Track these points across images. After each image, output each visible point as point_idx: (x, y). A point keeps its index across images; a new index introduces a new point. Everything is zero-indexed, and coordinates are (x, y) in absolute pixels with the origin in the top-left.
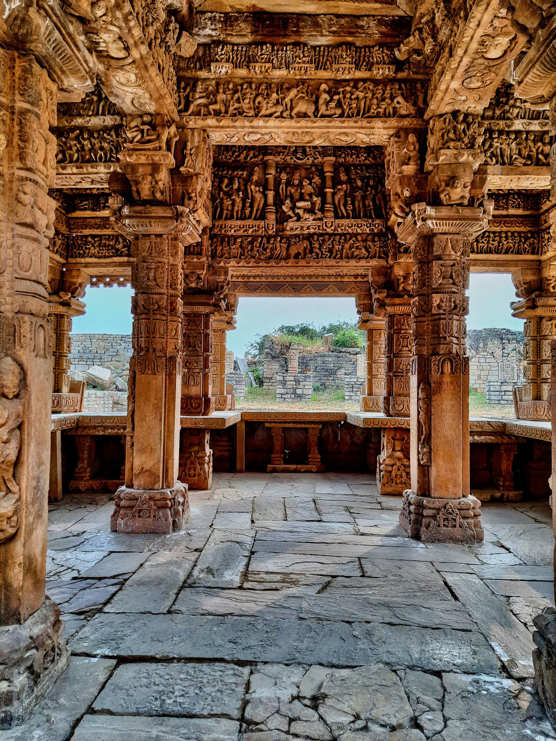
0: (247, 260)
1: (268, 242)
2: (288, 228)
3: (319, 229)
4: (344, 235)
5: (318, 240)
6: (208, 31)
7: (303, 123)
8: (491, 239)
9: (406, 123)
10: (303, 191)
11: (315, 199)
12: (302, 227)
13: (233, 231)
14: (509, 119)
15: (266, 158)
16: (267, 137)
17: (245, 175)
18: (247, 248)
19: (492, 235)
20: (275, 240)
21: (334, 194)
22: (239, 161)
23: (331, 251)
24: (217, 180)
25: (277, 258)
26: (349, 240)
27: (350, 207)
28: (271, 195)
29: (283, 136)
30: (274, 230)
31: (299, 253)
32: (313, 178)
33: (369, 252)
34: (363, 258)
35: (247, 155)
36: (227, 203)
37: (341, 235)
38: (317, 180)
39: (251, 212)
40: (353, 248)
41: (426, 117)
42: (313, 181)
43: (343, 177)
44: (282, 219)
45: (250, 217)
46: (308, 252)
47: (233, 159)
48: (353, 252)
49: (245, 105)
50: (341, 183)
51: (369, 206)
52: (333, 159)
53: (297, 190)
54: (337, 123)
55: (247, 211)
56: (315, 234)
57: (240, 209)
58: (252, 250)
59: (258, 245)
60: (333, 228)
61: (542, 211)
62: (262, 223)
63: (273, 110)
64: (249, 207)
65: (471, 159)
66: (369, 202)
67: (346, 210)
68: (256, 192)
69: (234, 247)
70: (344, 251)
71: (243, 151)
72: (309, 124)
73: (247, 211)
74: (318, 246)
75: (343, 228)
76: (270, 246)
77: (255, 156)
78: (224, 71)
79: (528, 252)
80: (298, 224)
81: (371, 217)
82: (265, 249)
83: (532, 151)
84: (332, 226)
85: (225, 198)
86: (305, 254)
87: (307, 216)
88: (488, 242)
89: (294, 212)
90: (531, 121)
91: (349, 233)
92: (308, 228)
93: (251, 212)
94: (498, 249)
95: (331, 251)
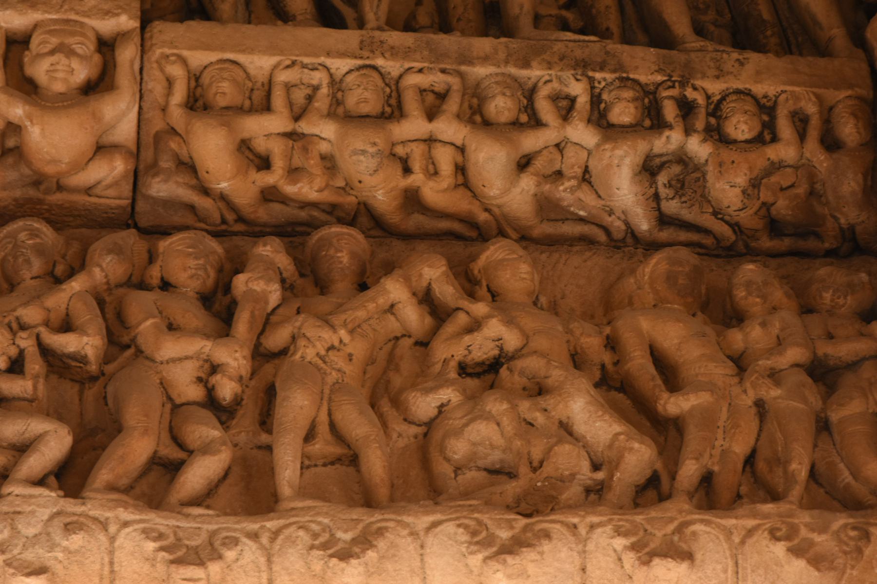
4: (295, 231)
33: (666, 432)
37: (236, 230)
40: (425, 377)
70: (297, 405)
84: (99, 85)
91: (362, 216)
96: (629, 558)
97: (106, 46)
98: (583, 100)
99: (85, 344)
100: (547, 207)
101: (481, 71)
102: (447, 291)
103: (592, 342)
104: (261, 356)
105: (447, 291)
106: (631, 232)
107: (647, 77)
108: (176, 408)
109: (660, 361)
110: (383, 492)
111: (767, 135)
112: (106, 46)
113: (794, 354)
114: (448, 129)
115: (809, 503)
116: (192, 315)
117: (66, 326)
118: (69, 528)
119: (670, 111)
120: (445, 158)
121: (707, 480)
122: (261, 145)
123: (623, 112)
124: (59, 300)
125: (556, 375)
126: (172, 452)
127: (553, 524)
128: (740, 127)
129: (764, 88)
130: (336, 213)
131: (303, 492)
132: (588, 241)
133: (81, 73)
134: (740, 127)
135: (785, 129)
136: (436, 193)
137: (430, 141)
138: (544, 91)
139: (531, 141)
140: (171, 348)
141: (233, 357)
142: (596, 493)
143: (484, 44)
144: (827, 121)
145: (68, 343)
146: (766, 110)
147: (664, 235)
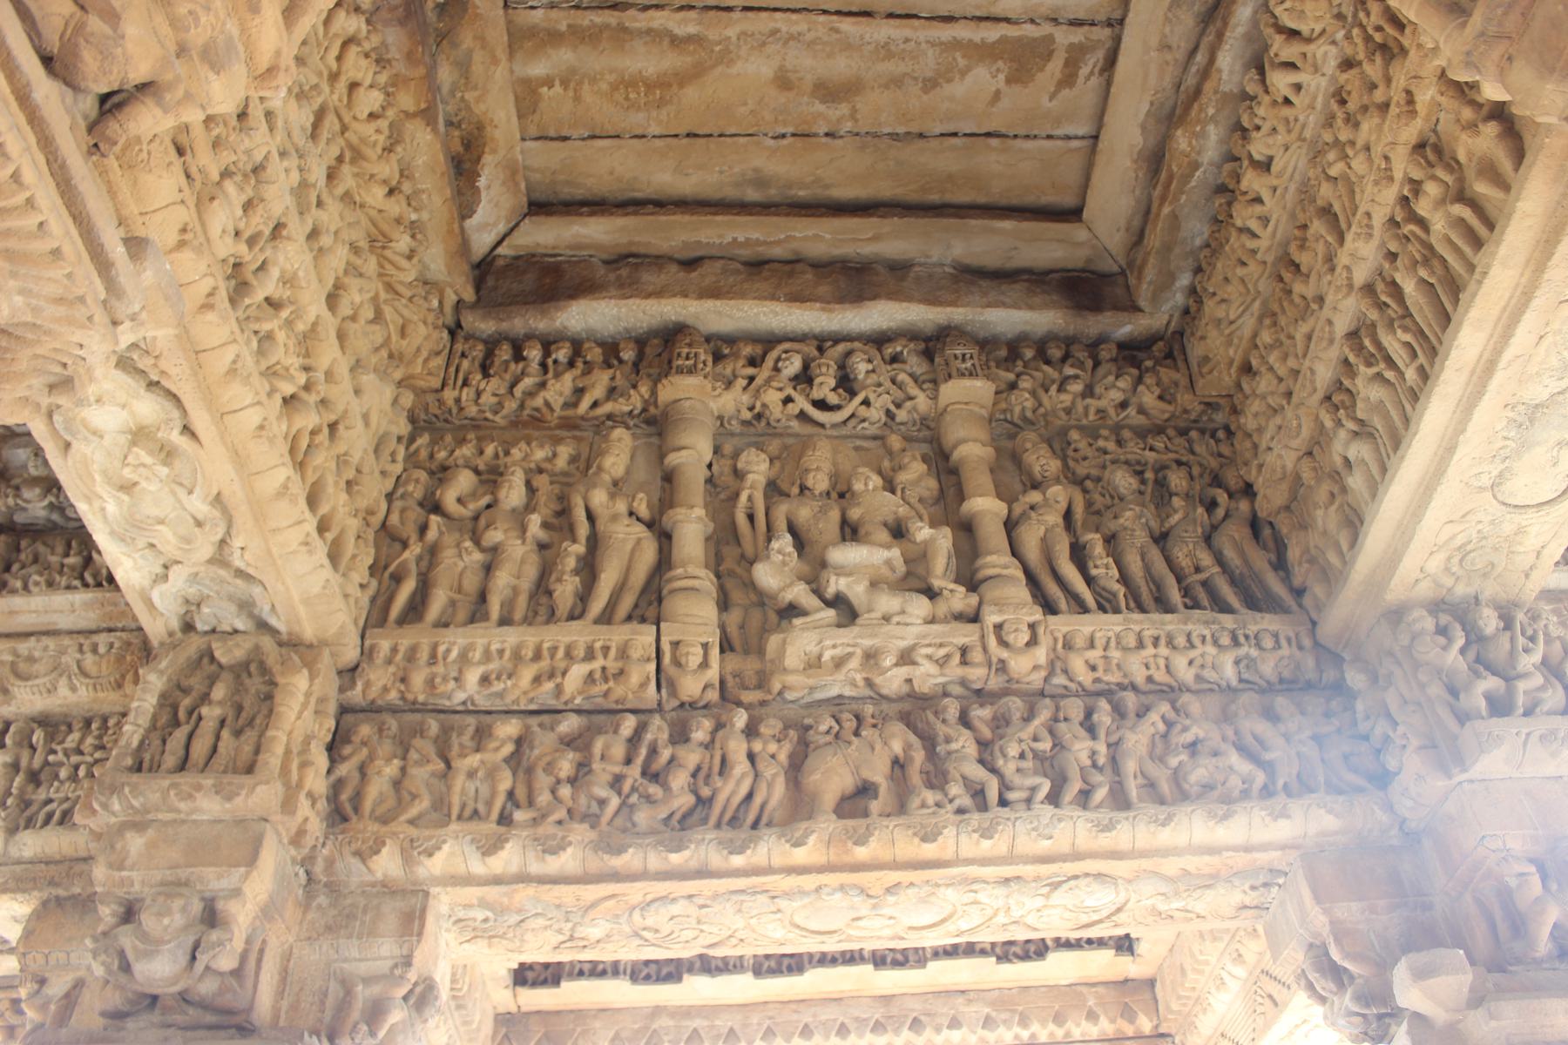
0: (548, 828)
1: (680, 735)
2: (793, 659)
3: (964, 662)
4: (1107, 694)
10: (854, 514)
12: (871, 657)
13: (472, 677)
17: (561, 463)
18: (549, 768)
20: (719, 726)
21: (1010, 525)
22: (537, 421)
23: (1052, 766)
24: (423, 476)
25: (734, 822)
28: (692, 529)
30: (713, 674)
31: (865, 790)
35: (579, 392)
36: (461, 561)
38: (914, 471)
39: (584, 597)
42: (903, 477)
43: (1042, 461)
47: (511, 405)
48: (1177, 776)
51: (1198, 570)
55: (566, 589)
57: (526, 585)
58: (583, 767)
59: (619, 751)
60: (1041, 654)
62: (644, 637)
64: (576, 572)
67: (1089, 581)
68: (615, 518)
69: (474, 760)
70: (1130, 766)
71: (557, 376)
73: (566, 589)
74: (972, 750)
75: (1094, 655)
76: (692, 757)
77: (612, 392)
80: (846, 636)
81: (1226, 609)
84: (1033, 642)
85: (449, 539)
87: (888, 602)
89: (818, 593)
92: (906, 658)
93: (584, 597)
95: (1052, 766)
96: (1268, 819)
97: (1032, 626)
98: (1208, 637)
99: (1045, 745)
100: (1199, 678)
101: (1169, 628)
102: (1171, 715)
103: (1230, 733)
104: (1109, 746)
105: (1171, 715)
106: (1229, 686)
109: (1256, 738)
110: (1169, 798)
111: (1278, 646)
112: (1032, 626)
113: (1308, 733)
114: (1163, 650)
116: (1083, 733)
117: (1035, 739)
118: (1060, 820)
119: (1242, 639)
120: (1162, 662)
121: (1285, 784)
122: (1092, 662)
123: (1225, 640)
125: (1223, 746)
126: (1086, 787)
127: (1237, 807)
128: (1268, 643)
130: (1122, 687)
131: (1141, 800)
132: (1211, 690)
133: (1025, 637)
134: (1268, 643)
135: (1284, 643)
136: (1160, 676)
137: (1155, 656)
138: (1194, 635)
139: (1193, 654)
140: (1077, 746)
141: (1102, 748)
142: (1245, 794)
144: (1297, 635)
145: (1040, 746)
146: (1276, 636)
147: (1242, 686)
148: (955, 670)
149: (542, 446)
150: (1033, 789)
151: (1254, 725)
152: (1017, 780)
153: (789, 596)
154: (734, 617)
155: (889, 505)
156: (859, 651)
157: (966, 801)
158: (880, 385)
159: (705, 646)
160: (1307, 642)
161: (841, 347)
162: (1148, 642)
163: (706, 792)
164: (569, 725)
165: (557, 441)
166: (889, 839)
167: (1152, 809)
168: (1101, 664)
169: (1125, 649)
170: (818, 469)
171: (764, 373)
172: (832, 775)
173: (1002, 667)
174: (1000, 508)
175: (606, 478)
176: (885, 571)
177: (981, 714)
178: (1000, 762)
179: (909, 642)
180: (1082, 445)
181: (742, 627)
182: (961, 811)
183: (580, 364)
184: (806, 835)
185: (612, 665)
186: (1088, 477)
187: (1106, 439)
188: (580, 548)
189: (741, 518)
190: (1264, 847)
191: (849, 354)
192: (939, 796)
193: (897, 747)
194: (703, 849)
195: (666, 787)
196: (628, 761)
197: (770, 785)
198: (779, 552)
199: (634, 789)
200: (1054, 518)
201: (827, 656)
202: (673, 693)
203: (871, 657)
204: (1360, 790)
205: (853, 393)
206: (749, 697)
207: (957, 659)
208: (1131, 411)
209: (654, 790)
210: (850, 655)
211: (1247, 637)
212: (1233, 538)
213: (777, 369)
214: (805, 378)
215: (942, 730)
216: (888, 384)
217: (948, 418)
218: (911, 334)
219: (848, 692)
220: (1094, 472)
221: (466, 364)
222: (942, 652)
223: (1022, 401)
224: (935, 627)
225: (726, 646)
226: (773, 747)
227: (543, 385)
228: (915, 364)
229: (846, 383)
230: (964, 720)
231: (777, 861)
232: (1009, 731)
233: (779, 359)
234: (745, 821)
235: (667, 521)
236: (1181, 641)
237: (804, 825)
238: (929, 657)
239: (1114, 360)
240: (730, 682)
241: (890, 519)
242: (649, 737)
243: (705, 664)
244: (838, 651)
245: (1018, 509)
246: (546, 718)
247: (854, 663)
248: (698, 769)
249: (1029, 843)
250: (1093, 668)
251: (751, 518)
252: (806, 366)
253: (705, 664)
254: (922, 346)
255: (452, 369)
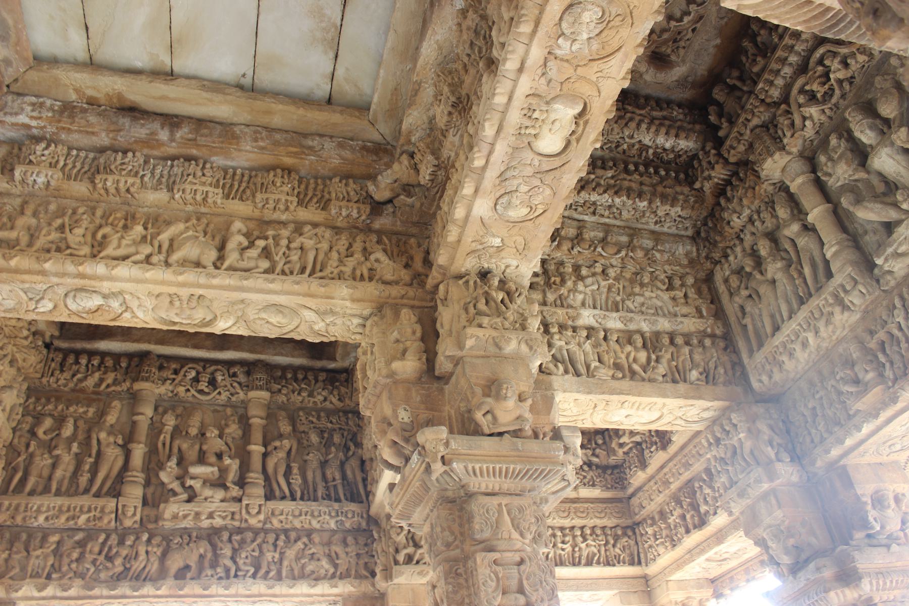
1: (121, 542)
2: (167, 515)
3: (232, 519)
4: (286, 532)
5: (230, 540)
6: (23, 119)
7: (190, 276)
8: (559, 540)
9: (395, 291)
10: (205, 447)
11: (227, 461)
12: (197, 514)
14: (570, 306)
15: (138, 386)
16: (115, 304)
17: (90, 414)
18: (69, 555)
19: (559, 533)
21: (265, 455)
22: (82, 391)
24: (29, 419)
25: (137, 578)
26: (296, 541)
27: (296, 481)
28: (139, 452)
29: (149, 303)
30: (138, 518)
31: (187, 567)
32: (227, 425)
33: (336, 566)
34: (324, 578)
35: (101, 380)
36: (43, 462)
37: (277, 533)
38: (233, 429)
39: (91, 481)
40: (303, 557)
41: (430, 282)
42: (227, 431)
43: (285, 427)
44: (155, 498)
45: (86, 491)
46: (207, 564)
47: (71, 385)
48: (303, 567)
49: (75, 237)
50: (281, 436)
51: (334, 480)
52: (265, 394)
53: (192, 446)
54: (259, 281)
55: (84, 480)
56: (225, 528)
57: (68, 475)
59: (96, 549)
60: (262, 517)
61: (630, 490)
62: (111, 504)
63: (132, 250)
64: (89, 471)
65: (524, 348)
66: (332, 472)
67: (289, 484)
68: (108, 445)
71: (93, 372)
72: (203, 280)
73: (84, 480)
75: (282, 518)
76: (124, 552)
77: (116, 382)
78: (41, 180)
79: (624, 563)
80: (189, 506)
81: (338, 500)
82: (109, 558)
83: (620, 358)
84: (259, 512)
85: (38, 452)
86: (201, 570)
87: (208, 492)
88: (554, 545)
89: (183, 485)
90: (607, 313)
92: (211, 516)
93: (91, 481)
94: (573, 558)
97: (260, 506)
102: (307, 542)
103: (327, 551)
105: (307, 542)
107: (337, 508)
108: (269, 563)
109: (336, 553)
111: (353, 517)
112: (260, 506)
114: (308, 517)
115: (356, 578)
116: (272, 548)
117: (253, 551)
123: (333, 514)
124: (252, 547)
125: (321, 558)
127: (319, 582)
128: (350, 515)
129: (354, 509)
131: (287, 577)
133: (256, 511)
134: (350, 515)
141: (277, 556)
143: (314, 503)
145: (254, 554)
148: (228, 521)
149: (82, 407)
150: (248, 571)
151: (337, 548)
152: (243, 567)
153: (170, 487)
154: (150, 490)
155: (217, 444)
156: (193, 513)
157: (223, 575)
158: (226, 386)
159: (135, 507)
160: (365, 516)
161: (213, 368)
162: (303, 514)
163: (128, 566)
164: (79, 536)
165: (88, 406)
166: (192, 587)
167: (289, 582)
168: (284, 521)
169: (294, 516)
170: (194, 426)
171: (179, 378)
172: (175, 562)
173: (246, 521)
174: (263, 449)
175: (108, 424)
176: (211, 476)
177: (237, 538)
178: (238, 560)
179: (214, 508)
180: (303, 418)
181: (154, 494)
182: (220, 578)
183: (103, 369)
184: (161, 586)
185: (98, 515)
186: (304, 432)
187: (313, 416)
188: (92, 460)
189: (160, 445)
190: (329, 595)
191: (216, 370)
192: (213, 572)
193: (202, 551)
194: (124, 588)
195: (112, 562)
196: (100, 553)
197: (152, 564)
198: (170, 467)
199: (101, 564)
200: (282, 454)
201: (181, 514)
202: (121, 524)
203: (197, 514)
204: (366, 577)
205: (215, 390)
206: (151, 526)
207: (229, 517)
208: (327, 403)
209: (109, 565)
210: (189, 514)
211: (342, 513)
212: (352, 466)
213: (185, 376)
214: (196, 380)
215: (220, 544)
216: (229, 386)
217: (251, 404)
218: (242, 363)
219: (188, 526)
220: (306, 430)
221: (53, 365)
222: (224, 514)
223: (282, 398)
224: (224, 504)
225: (145, 503)
226: (155, 549)
227: (85, 378)
228: (242, 378)
229: (213, 383)
230: (230, 540)
231: (151, 593)
232: (245, 546)
233: (186, 371)
234: (141, 578)
235: (130, 446)
236: (316, 514)
237: (161, 582)
238: (220, 516)
239: (324, 381)
240: (145, 519)
241: (218, 451)
242: (109, 543)
243: (134, 514)
244: (185, 512)
245: (270, 448)
246: (70, 533)
247: (190, 518)
248: (127, 556)
249: (242, 591)
250: (282, 522)
251: (164, 444)
252: (198, 373)
253: (134, 514)
254: (246, 369)
255: (47, 368)
